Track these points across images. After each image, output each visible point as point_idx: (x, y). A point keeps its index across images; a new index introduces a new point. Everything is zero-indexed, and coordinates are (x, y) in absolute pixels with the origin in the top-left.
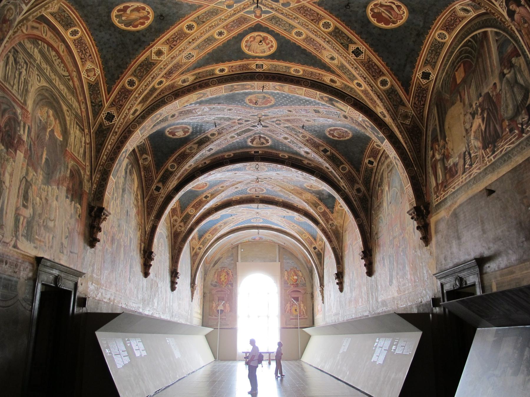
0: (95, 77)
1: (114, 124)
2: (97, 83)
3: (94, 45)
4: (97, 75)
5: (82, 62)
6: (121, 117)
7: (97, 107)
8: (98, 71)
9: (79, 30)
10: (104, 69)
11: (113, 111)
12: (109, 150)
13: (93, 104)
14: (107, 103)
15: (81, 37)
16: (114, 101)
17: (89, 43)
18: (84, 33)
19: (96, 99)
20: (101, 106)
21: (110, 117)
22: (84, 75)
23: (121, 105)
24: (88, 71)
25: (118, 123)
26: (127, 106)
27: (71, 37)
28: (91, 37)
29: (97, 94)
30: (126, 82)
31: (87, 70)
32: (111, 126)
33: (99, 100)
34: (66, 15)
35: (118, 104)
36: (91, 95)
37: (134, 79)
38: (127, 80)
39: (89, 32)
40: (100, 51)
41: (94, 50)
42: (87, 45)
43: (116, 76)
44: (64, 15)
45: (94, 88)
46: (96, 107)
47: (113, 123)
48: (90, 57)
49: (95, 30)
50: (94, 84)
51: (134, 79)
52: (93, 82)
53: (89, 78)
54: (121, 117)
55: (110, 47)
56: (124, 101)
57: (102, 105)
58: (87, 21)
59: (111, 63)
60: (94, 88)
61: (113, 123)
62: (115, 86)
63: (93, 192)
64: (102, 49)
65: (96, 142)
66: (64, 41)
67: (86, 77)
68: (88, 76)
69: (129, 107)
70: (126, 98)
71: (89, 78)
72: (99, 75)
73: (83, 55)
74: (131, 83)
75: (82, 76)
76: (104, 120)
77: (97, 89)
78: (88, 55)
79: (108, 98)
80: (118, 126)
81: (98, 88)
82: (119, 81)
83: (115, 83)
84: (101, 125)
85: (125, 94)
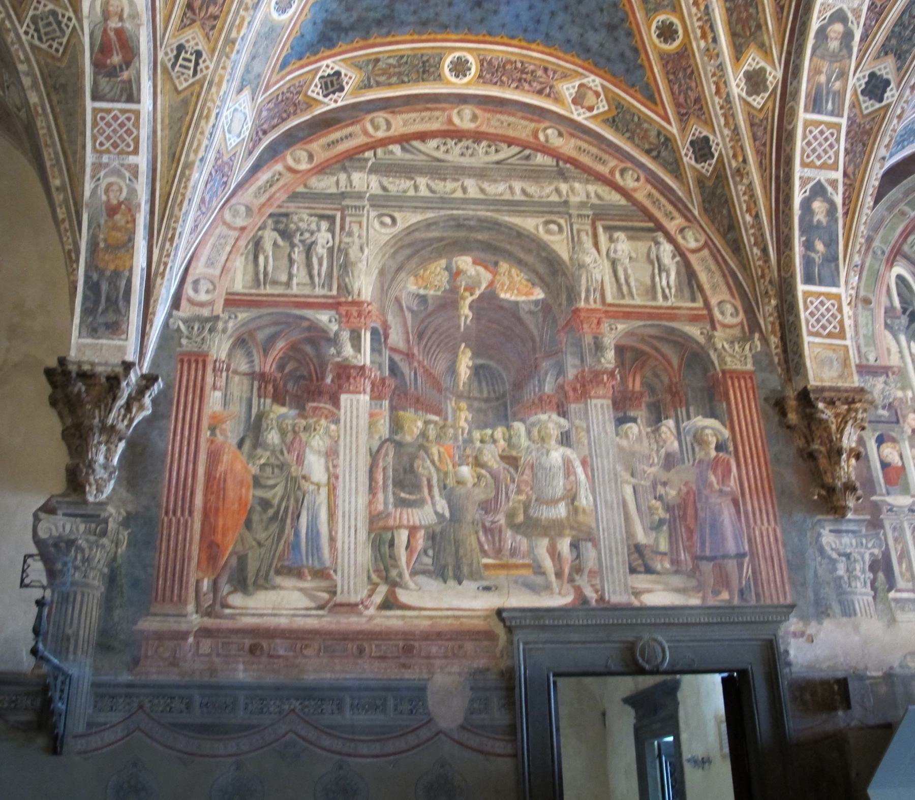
0: (602, 96)
1: (721, 155)
2: (617, 105)
3: (523, 44)
4: (599, 89)
5: (549, 95)
6: (719, 125)
7: (661, 150)
8: (594, 81)
9: (457, 54)
10: (596, 65)
11: (697, 130)
12: (753, 227)
13: (654, 153)
14: (669, 123)
15: (481, 62)
16: (678, 105)
17: (512, 53)
18: (477, 49)
19: (645, 137)
20: (668, 141)
21: (702, 149)
22: (580, 116)
23: (697, 100)
24: (578, 100)
25: (726, 148)
26: (709, 88)
27: (466, 80)
28: (498, 39)
29: (639, 125)
30: (656, 41)
31: (575, 101)
32: (719, 165)
33: (653, 134)
34: (391, 61)
35: (691, 107)
36: (631, 139)
37: (662, 17)
38: (654, 37)
39: (480, 38)
40: (548, 40)
41: (536, 55)
42: (513, 58)
43: (629, 54)
44: (390, 65)
45: (620, 118)
46: (664, 153)
47: (716, 155)
48: (551, 74)
49: (482, 21)
50: (615, 113)
51: (662, 17)
52: (610, 110)
53: (595, 112)
54: (719, 125)
55: (553, 14)
56: (693, 84)
57: (667, 139)
58: (444, 27)
59: (594, 39)
60: (620, 118)
61: (716, 155)
62: (649, 73)
63: (776, 359)
64: (547, 35)
65: (718, 231)
66: (463, 99)
67: (588, 114)
68: (590, 109)
69: (713, 88)
70: (692, 74)
71: (595, 112)
72: (603, 87)
73: (535, 84)
74: (667, 32)
75: (580, 119)
76: (698, 166)
77: (628, 117)
78: (540, 73)
79: (662, 113)
80: (731, 153)
81: (628, 111)
82: (643, 56)
83: (641, 66)
84: (700, 181)
85: (680, 66)
